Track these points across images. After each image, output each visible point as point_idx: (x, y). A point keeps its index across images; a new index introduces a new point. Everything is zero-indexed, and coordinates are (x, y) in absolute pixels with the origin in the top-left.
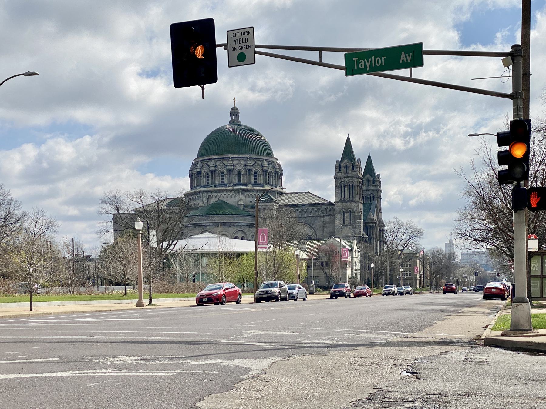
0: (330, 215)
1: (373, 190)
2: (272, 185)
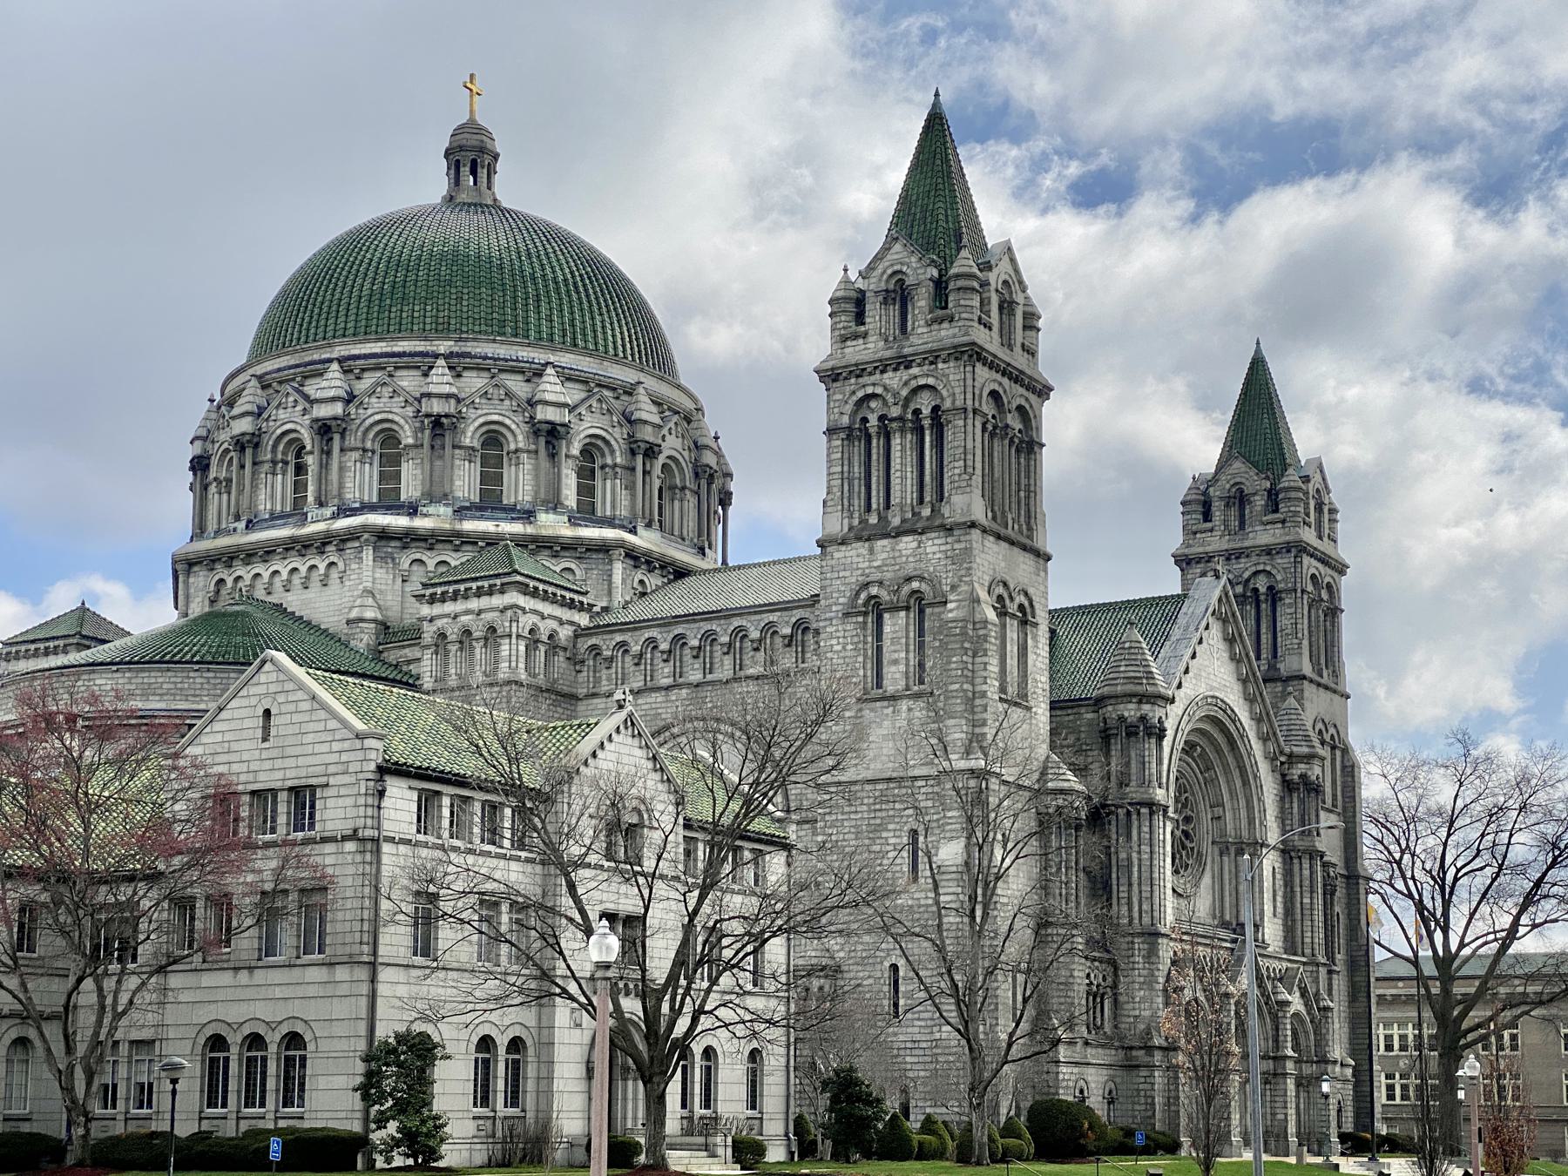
1: (1268, 551)
2: (610, 522)
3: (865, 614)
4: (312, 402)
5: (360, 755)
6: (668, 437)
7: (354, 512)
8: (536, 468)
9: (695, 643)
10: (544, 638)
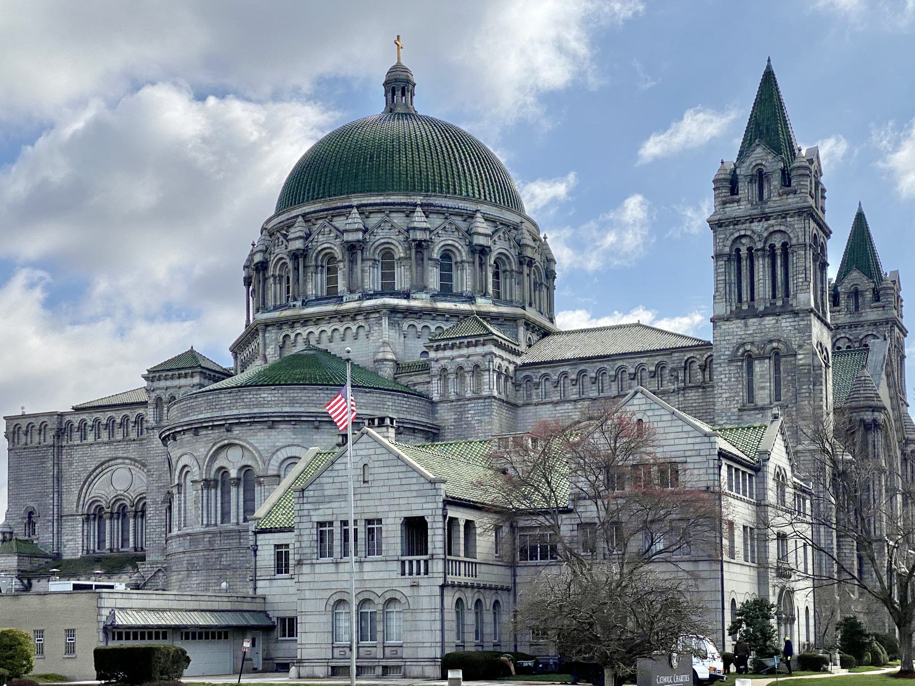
0: (703, 386)
1: (875, 324)
2: (510, 303)
3: (742, 361)
4: (343, 232)
5: (709, 446)
7: (370, 297)
9: (593, 375)
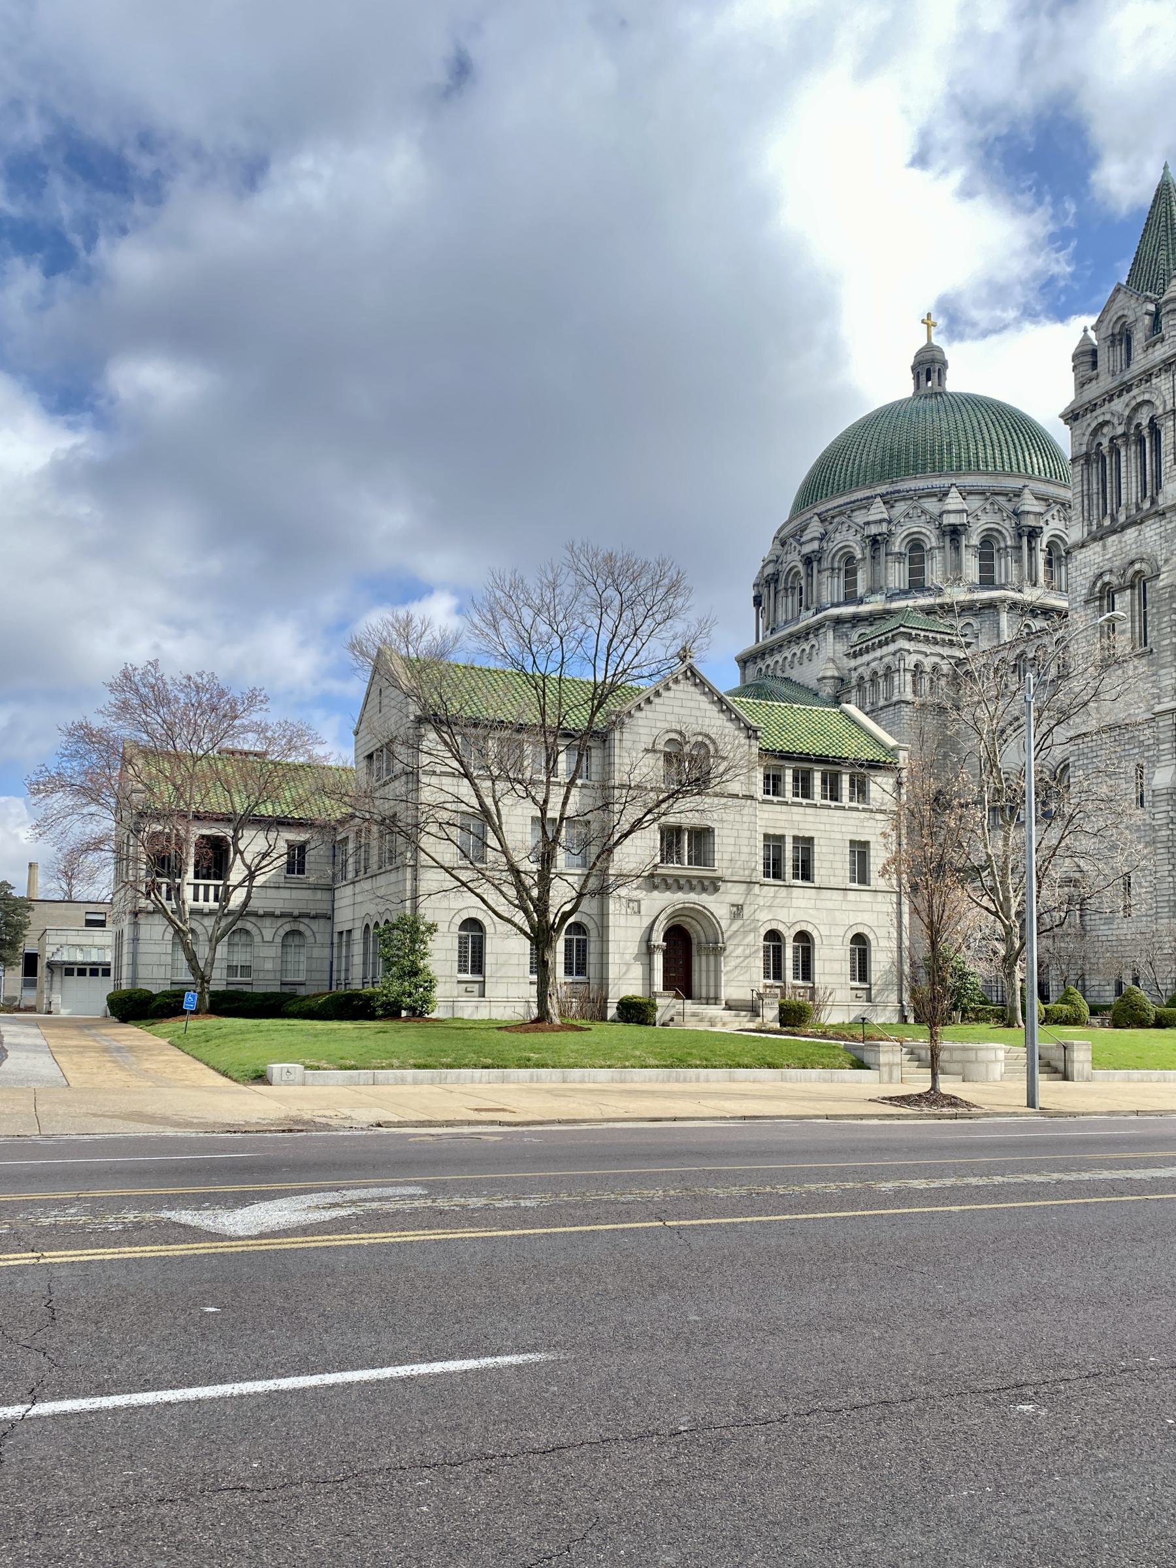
3: (1101, 599)
6: (1051, 522)
8: (944, 559)
10: (928, 669)
